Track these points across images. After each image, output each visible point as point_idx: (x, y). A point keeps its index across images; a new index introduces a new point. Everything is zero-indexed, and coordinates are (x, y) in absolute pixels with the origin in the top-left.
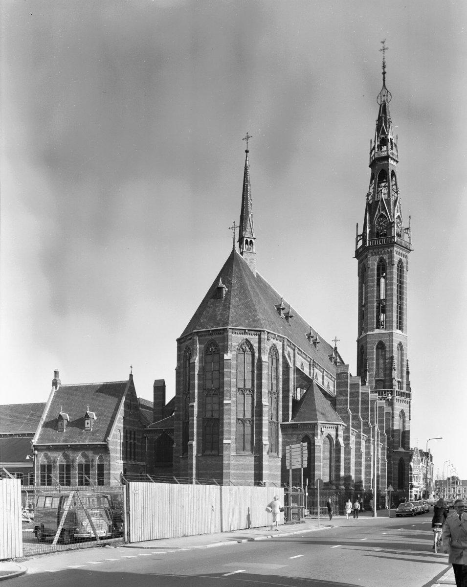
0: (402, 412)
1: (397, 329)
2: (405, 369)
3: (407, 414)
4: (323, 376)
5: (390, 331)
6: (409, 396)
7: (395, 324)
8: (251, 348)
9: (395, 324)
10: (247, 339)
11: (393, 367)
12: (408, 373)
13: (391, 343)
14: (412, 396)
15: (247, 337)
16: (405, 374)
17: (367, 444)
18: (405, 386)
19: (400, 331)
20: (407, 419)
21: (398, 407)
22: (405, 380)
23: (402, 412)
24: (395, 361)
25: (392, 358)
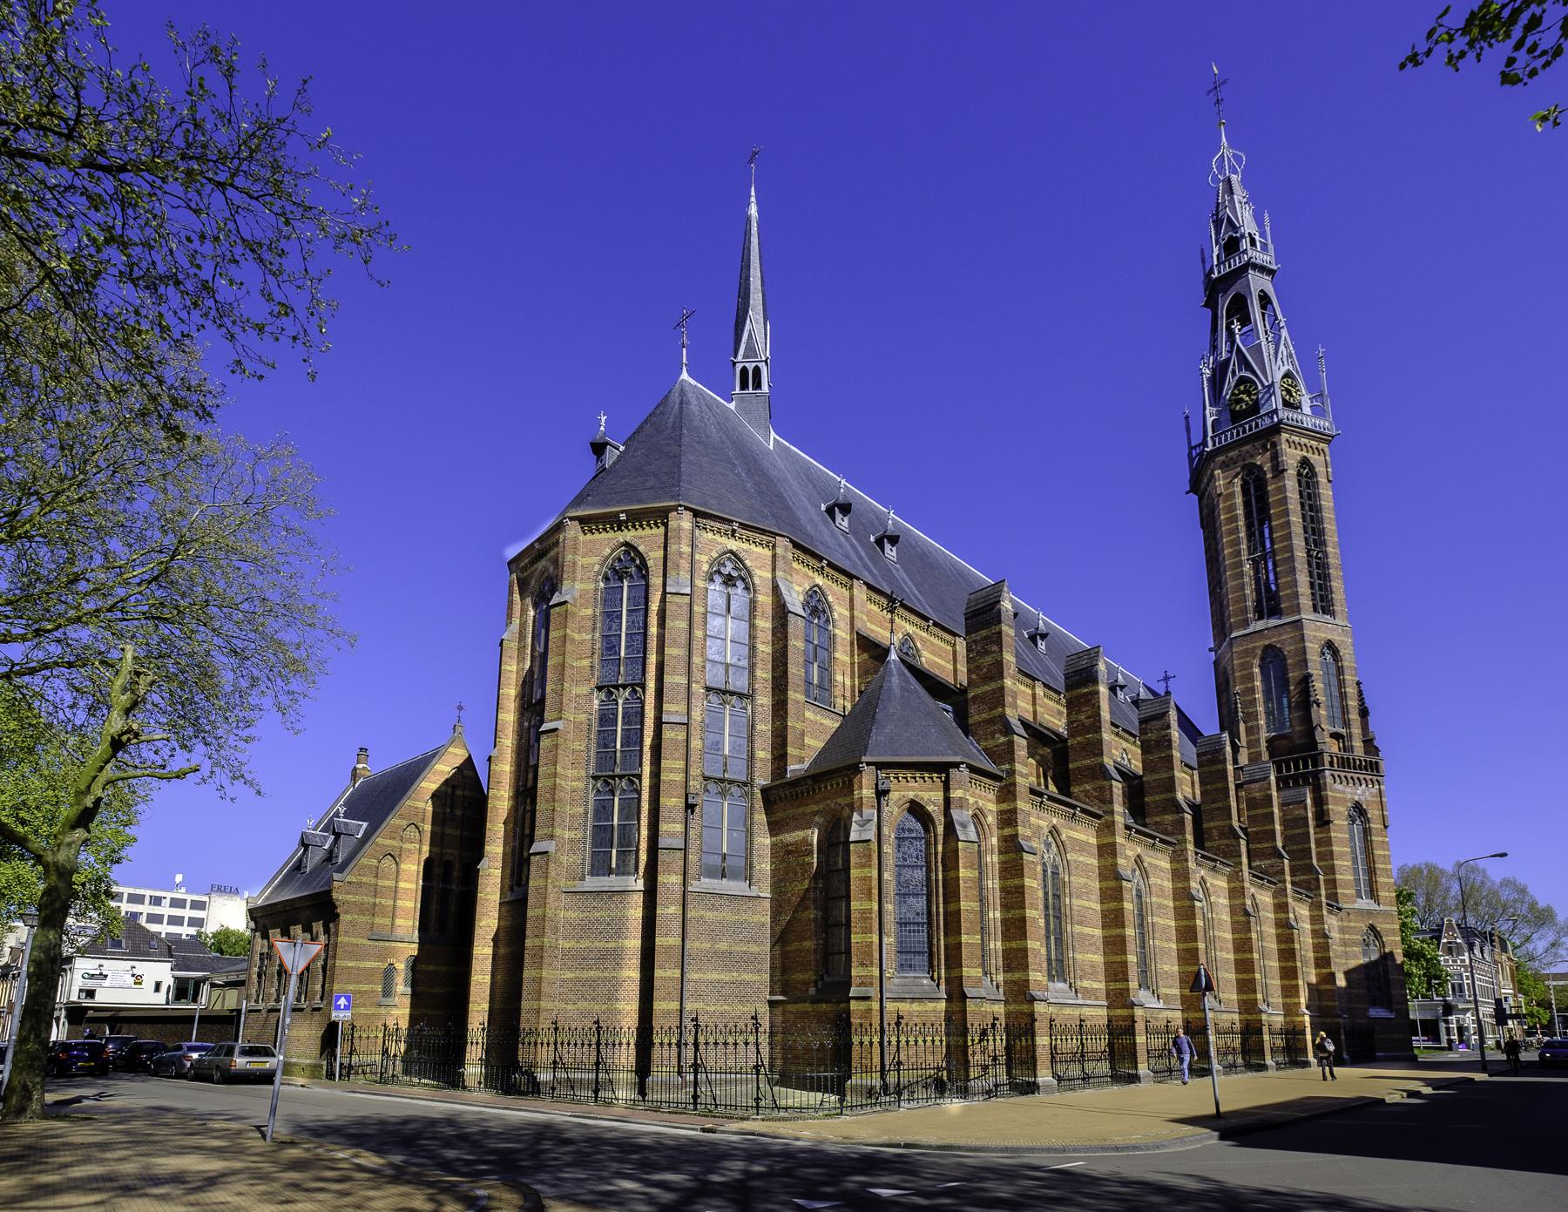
0: (1359, 810)
1: (1315, 610)
2: (1353, 703)
3: (1373, 813)
4: (1034, 696)
5: (1297, 618)
6: (1374, 767)
7: (1305, 601)
8: (643, 567)
9: (1305, 601)
10: (627, 544)
11: (1312, 699)
12: (1364, 713)
13: (1301, 645)
14: (1382, 765)
15: (628, 535)
16: (1354, 716)
17: (1316, 913)
18: (1358, 744)
19: (1329, 617)
20: (1376, 826)
21: (1342, 793)
22: (1356, 730)
23: (1359, 810)
24: (1318, 685)
25: (1306, 680)
